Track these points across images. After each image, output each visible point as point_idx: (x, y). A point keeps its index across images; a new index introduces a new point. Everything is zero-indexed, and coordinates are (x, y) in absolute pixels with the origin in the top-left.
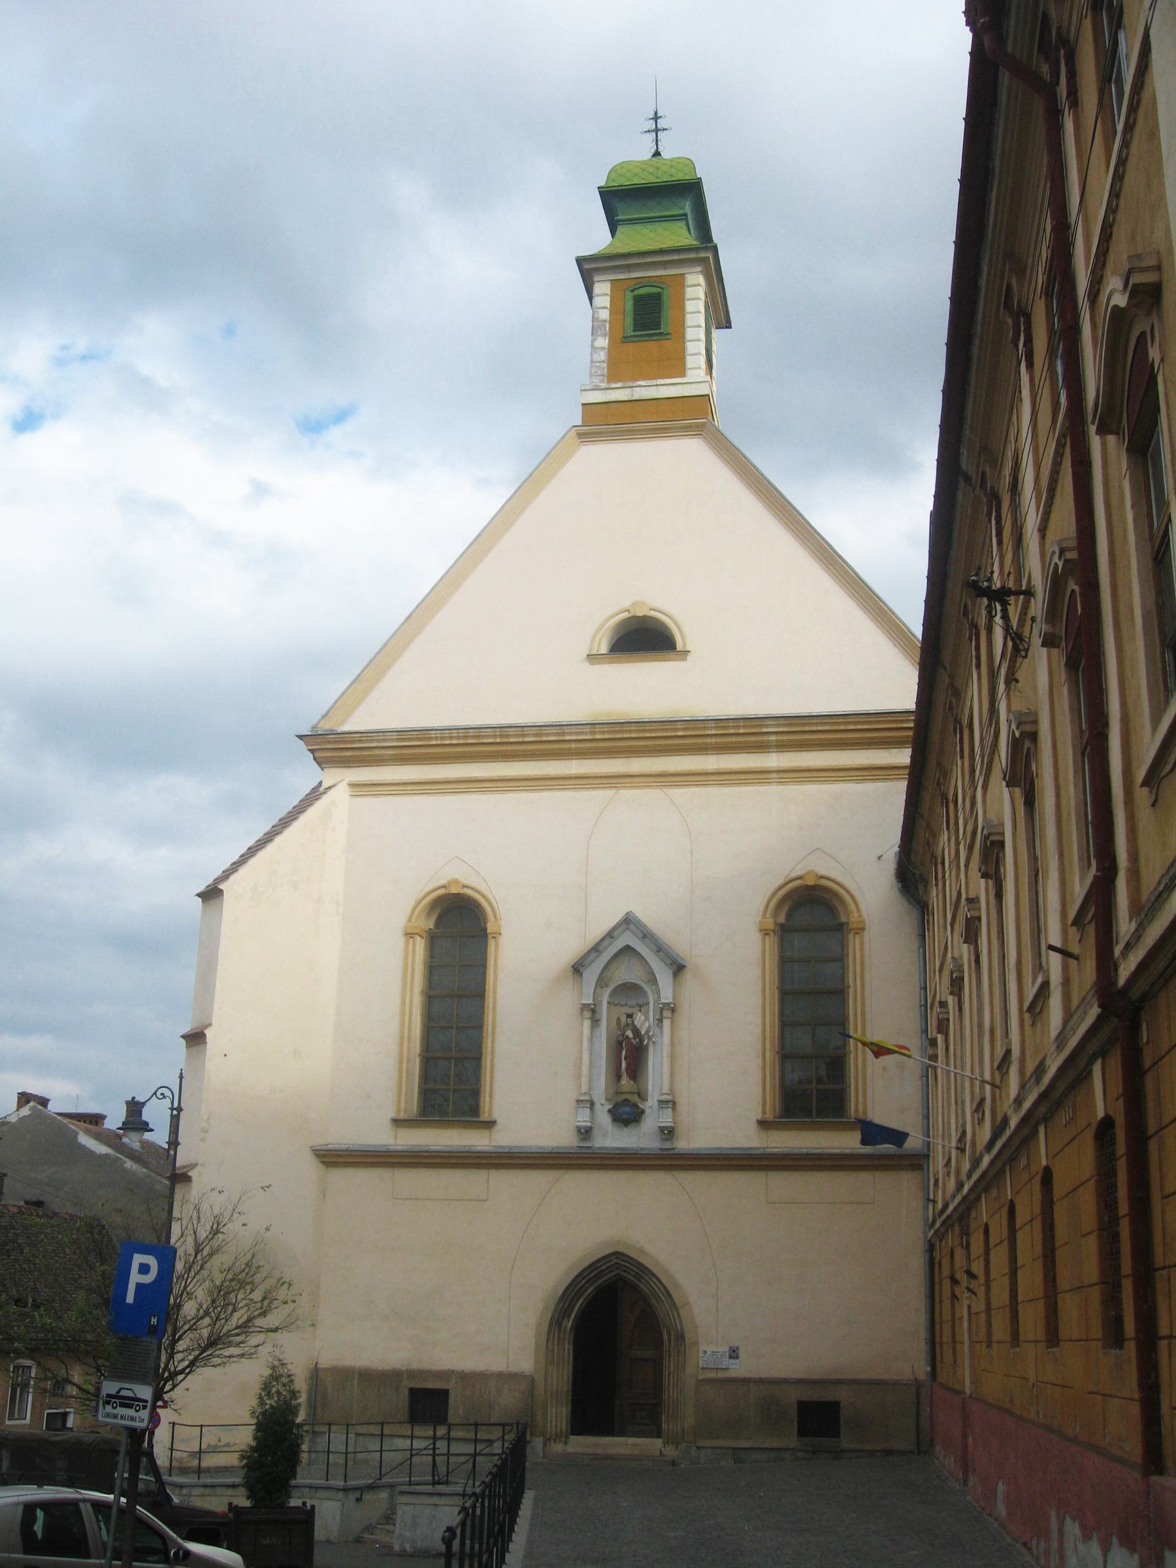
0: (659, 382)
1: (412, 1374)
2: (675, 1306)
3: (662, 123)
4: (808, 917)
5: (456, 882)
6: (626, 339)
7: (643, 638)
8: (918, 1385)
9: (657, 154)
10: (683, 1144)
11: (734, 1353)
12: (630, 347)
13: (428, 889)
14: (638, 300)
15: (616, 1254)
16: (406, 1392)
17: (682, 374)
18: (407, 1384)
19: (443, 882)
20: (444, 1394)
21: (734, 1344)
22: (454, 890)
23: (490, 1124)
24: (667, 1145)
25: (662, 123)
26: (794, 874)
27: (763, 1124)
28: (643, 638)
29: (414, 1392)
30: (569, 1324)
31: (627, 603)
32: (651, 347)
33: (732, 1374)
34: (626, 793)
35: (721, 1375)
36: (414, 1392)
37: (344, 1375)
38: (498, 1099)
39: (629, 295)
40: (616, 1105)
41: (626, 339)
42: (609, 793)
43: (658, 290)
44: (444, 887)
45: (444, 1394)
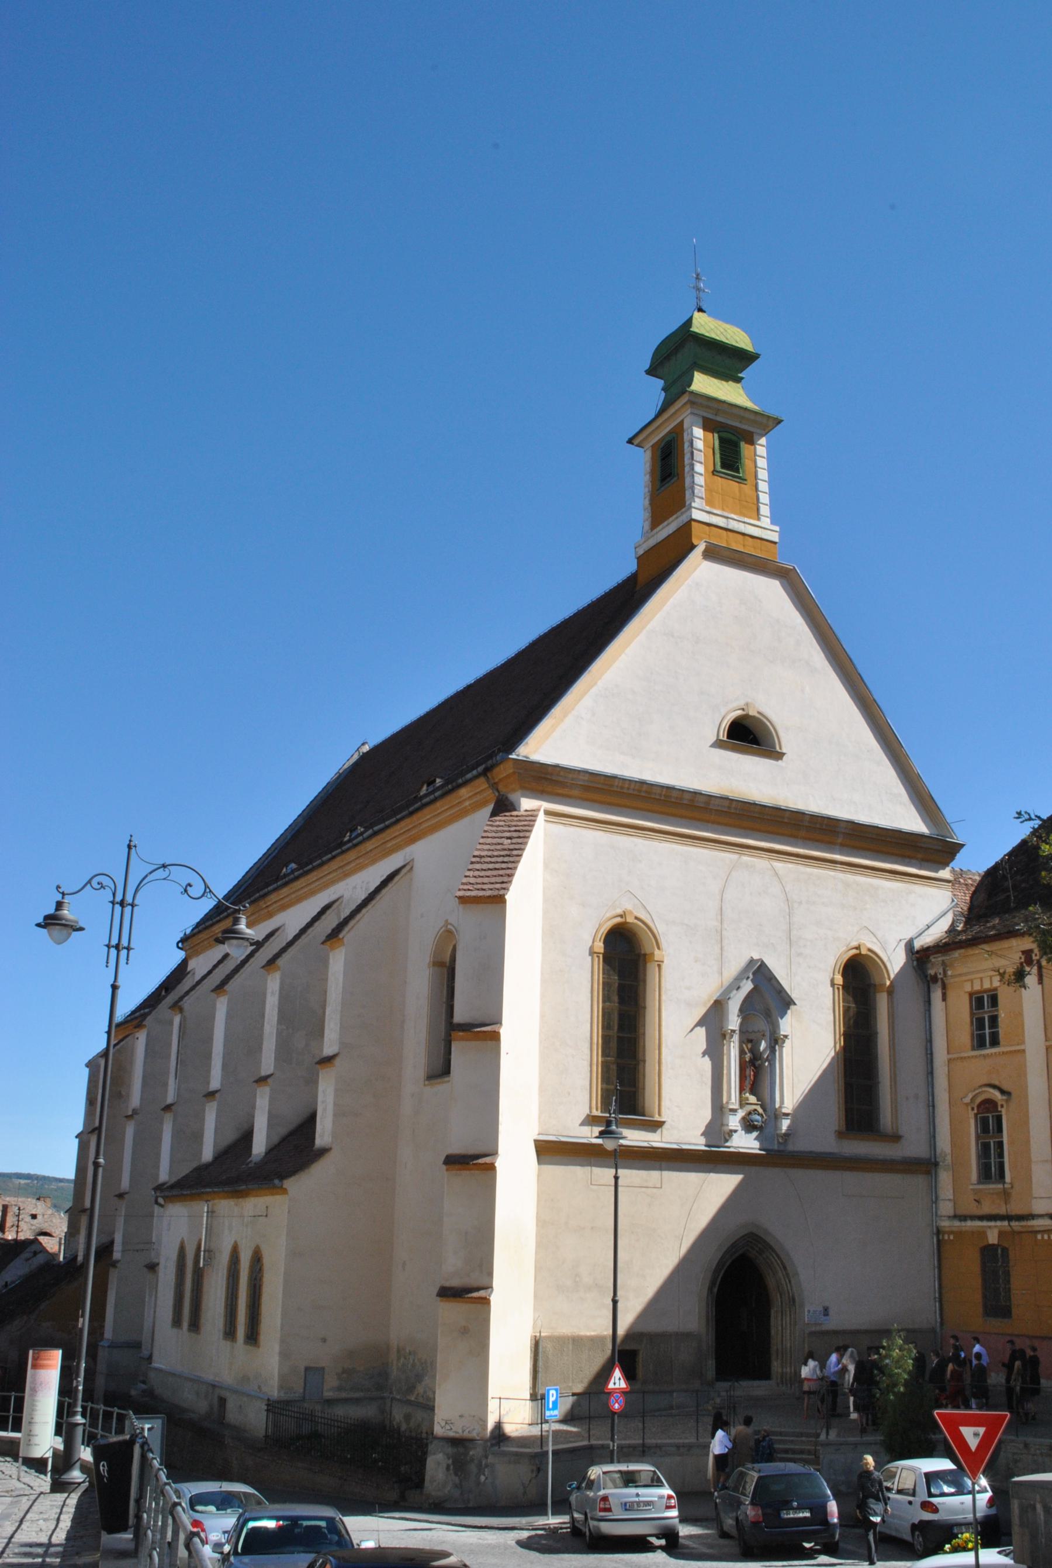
0: (746, 520)
2: (787, 1274)
4: (858, 975)
5: (631, 912)
6: (714, 472)
7: (747, 734)
8: (933, 1330)
10: (791, 1147)
11: (826, 1311)
13: (608, 915)
15: (752, 1233)
19: (619, 911)
21: (827, 1304)
22: (630, 919)
23: (659, 1125)
24: (782, 1148)
26: (855, 944)
27: (840, 1135)
28: (747, 734)
30: (715, 1290)
31: (741, 703)
33: (825, 1328)
34: (745, 859)
35: (818, 1328)
37: (561, 1341)
38: (665, 1103)
40: (750, 1113)
41: (714, 472)
42: (735, 857)
44: (621, 916)
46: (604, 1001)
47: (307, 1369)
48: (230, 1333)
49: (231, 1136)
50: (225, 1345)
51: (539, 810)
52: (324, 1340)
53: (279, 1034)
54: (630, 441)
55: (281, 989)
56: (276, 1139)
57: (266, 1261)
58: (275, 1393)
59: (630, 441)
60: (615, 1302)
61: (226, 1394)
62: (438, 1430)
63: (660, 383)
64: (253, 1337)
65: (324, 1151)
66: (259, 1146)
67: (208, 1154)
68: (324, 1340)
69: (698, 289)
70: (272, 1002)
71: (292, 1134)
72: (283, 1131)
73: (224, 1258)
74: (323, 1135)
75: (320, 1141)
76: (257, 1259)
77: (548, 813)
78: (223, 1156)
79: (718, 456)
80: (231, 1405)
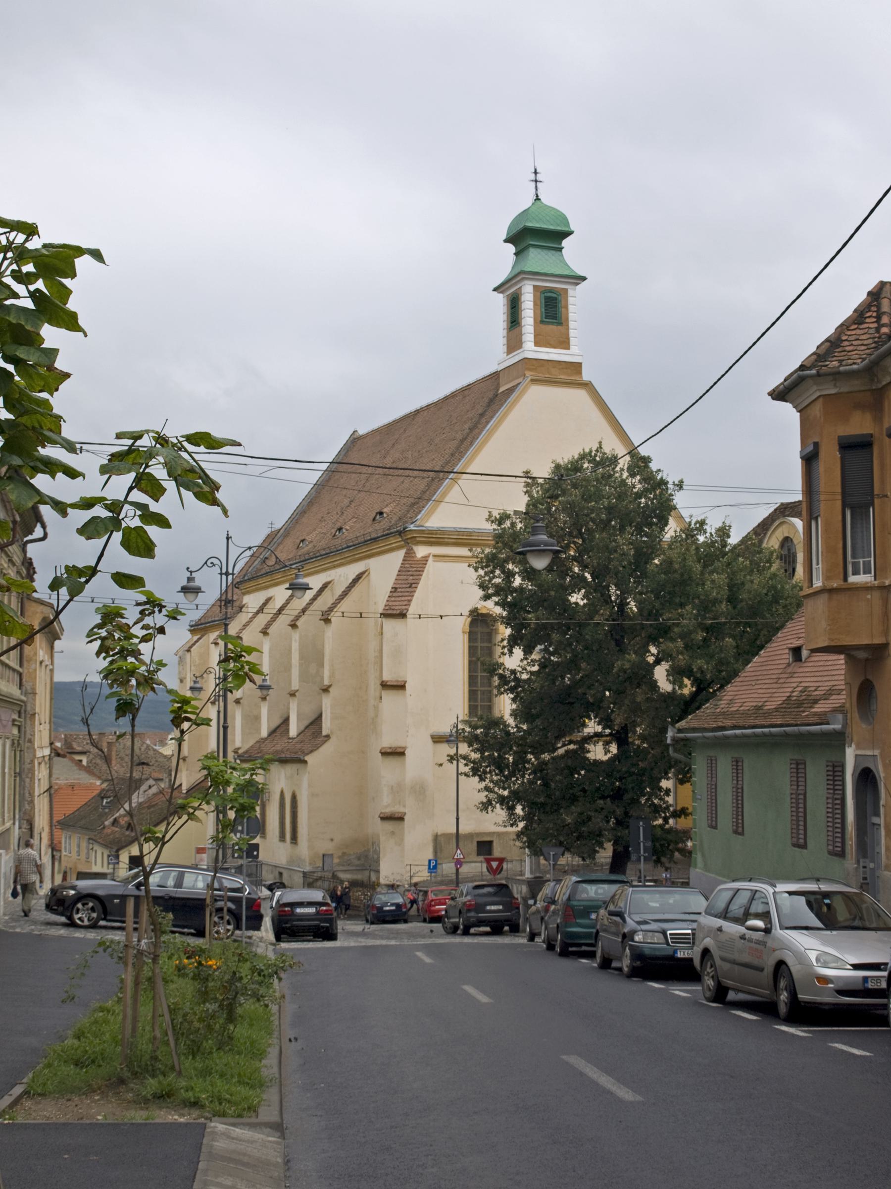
1: (478, 834)
3: (539, 177)
6: (542, 322)
9: (537, 199)
12: (543, 326)
14: (546, 298)
16: (475, 844)
17: (568, 348)
18: (476, 839)
20: (490, 843)
25: (539, 177)
29: (478, 842)
32: (551, 328)
36: (478, 842)
39: (543, 296)
43: (555, 295)
45: (490, 843)
46: (470, 657)
47: (324, 855)
48: (282, 837)
49: (277, 722)
50: (281, 844)
51: (428, 556)
52: (332, 840)
53: (301, 665)
54: (495, 290)
55: (300, 638)
56: (302, 728)
57: (298, 798)
58: (308, 869)
59: (495, 290)
60: (458, 819)
61: (282, 870)
62: (382, 881)
63: (511, 248)
64: (294, 838)
65: (328, 737)
66: (293, 731)
67: (264, 733)
68: (332, 840)
69: (536, 181)
70: (295, 646)
71: (311, 724)
72: (306, 723)
73: (276, 797)
74: (327, 726)
75: (324, 733)
76: (294, 798)
77: (434, 556)
78: (272, 733)
79: (543, 310)
80: (285, 876)
